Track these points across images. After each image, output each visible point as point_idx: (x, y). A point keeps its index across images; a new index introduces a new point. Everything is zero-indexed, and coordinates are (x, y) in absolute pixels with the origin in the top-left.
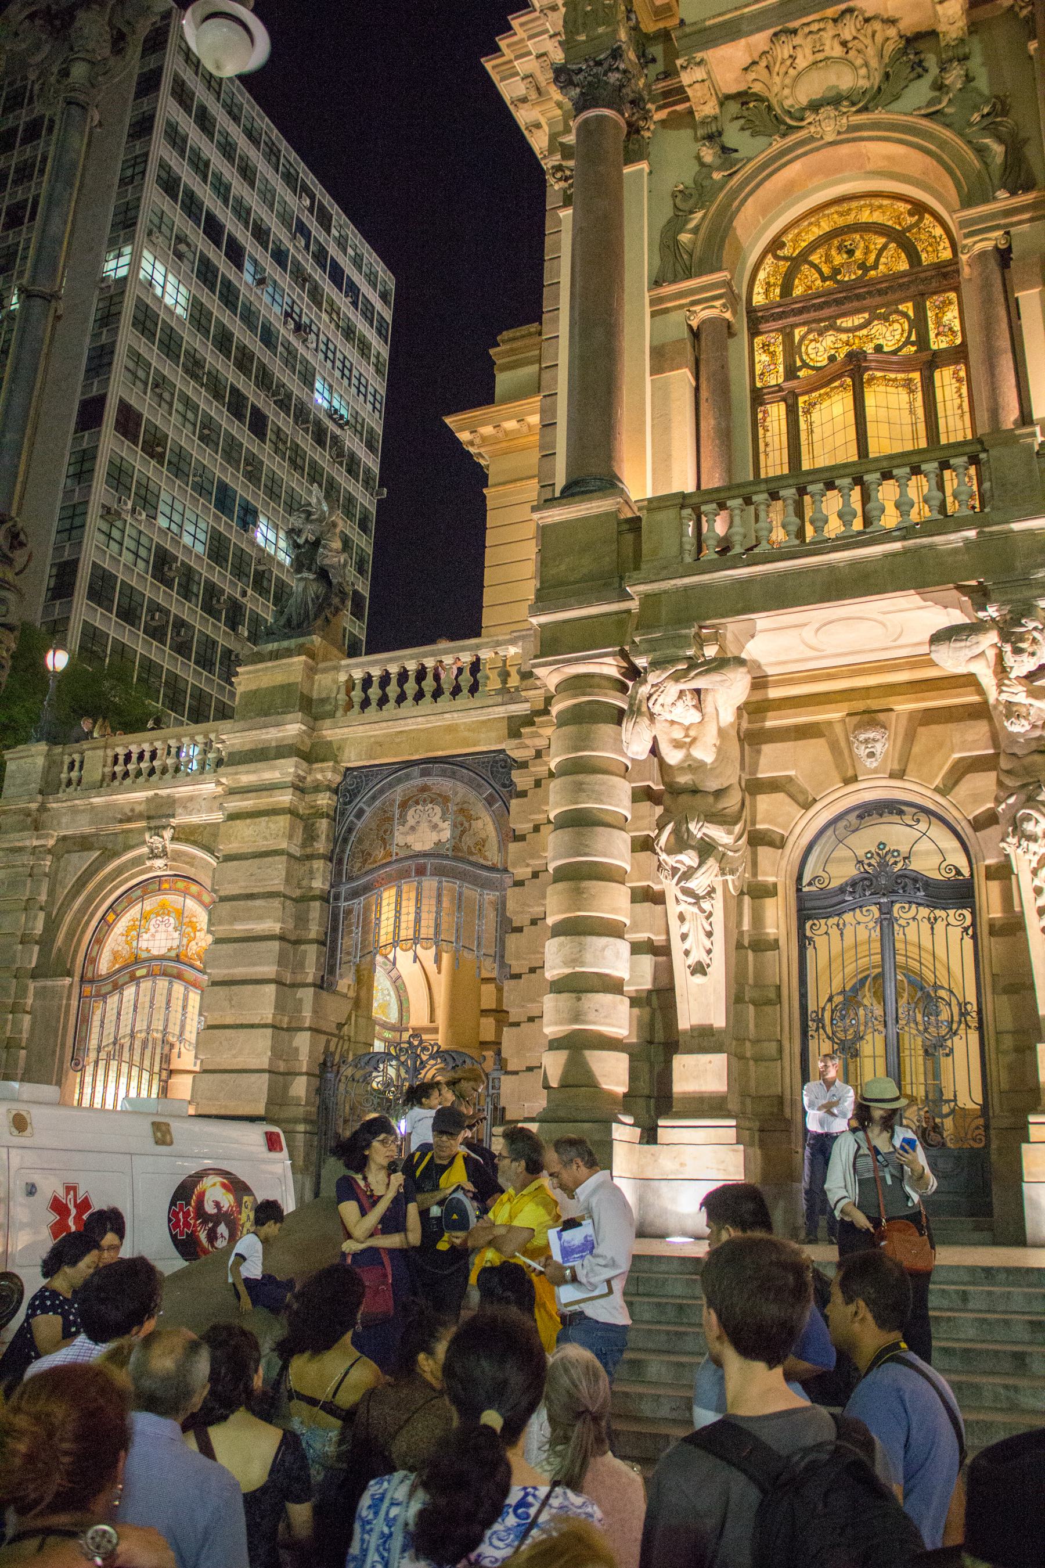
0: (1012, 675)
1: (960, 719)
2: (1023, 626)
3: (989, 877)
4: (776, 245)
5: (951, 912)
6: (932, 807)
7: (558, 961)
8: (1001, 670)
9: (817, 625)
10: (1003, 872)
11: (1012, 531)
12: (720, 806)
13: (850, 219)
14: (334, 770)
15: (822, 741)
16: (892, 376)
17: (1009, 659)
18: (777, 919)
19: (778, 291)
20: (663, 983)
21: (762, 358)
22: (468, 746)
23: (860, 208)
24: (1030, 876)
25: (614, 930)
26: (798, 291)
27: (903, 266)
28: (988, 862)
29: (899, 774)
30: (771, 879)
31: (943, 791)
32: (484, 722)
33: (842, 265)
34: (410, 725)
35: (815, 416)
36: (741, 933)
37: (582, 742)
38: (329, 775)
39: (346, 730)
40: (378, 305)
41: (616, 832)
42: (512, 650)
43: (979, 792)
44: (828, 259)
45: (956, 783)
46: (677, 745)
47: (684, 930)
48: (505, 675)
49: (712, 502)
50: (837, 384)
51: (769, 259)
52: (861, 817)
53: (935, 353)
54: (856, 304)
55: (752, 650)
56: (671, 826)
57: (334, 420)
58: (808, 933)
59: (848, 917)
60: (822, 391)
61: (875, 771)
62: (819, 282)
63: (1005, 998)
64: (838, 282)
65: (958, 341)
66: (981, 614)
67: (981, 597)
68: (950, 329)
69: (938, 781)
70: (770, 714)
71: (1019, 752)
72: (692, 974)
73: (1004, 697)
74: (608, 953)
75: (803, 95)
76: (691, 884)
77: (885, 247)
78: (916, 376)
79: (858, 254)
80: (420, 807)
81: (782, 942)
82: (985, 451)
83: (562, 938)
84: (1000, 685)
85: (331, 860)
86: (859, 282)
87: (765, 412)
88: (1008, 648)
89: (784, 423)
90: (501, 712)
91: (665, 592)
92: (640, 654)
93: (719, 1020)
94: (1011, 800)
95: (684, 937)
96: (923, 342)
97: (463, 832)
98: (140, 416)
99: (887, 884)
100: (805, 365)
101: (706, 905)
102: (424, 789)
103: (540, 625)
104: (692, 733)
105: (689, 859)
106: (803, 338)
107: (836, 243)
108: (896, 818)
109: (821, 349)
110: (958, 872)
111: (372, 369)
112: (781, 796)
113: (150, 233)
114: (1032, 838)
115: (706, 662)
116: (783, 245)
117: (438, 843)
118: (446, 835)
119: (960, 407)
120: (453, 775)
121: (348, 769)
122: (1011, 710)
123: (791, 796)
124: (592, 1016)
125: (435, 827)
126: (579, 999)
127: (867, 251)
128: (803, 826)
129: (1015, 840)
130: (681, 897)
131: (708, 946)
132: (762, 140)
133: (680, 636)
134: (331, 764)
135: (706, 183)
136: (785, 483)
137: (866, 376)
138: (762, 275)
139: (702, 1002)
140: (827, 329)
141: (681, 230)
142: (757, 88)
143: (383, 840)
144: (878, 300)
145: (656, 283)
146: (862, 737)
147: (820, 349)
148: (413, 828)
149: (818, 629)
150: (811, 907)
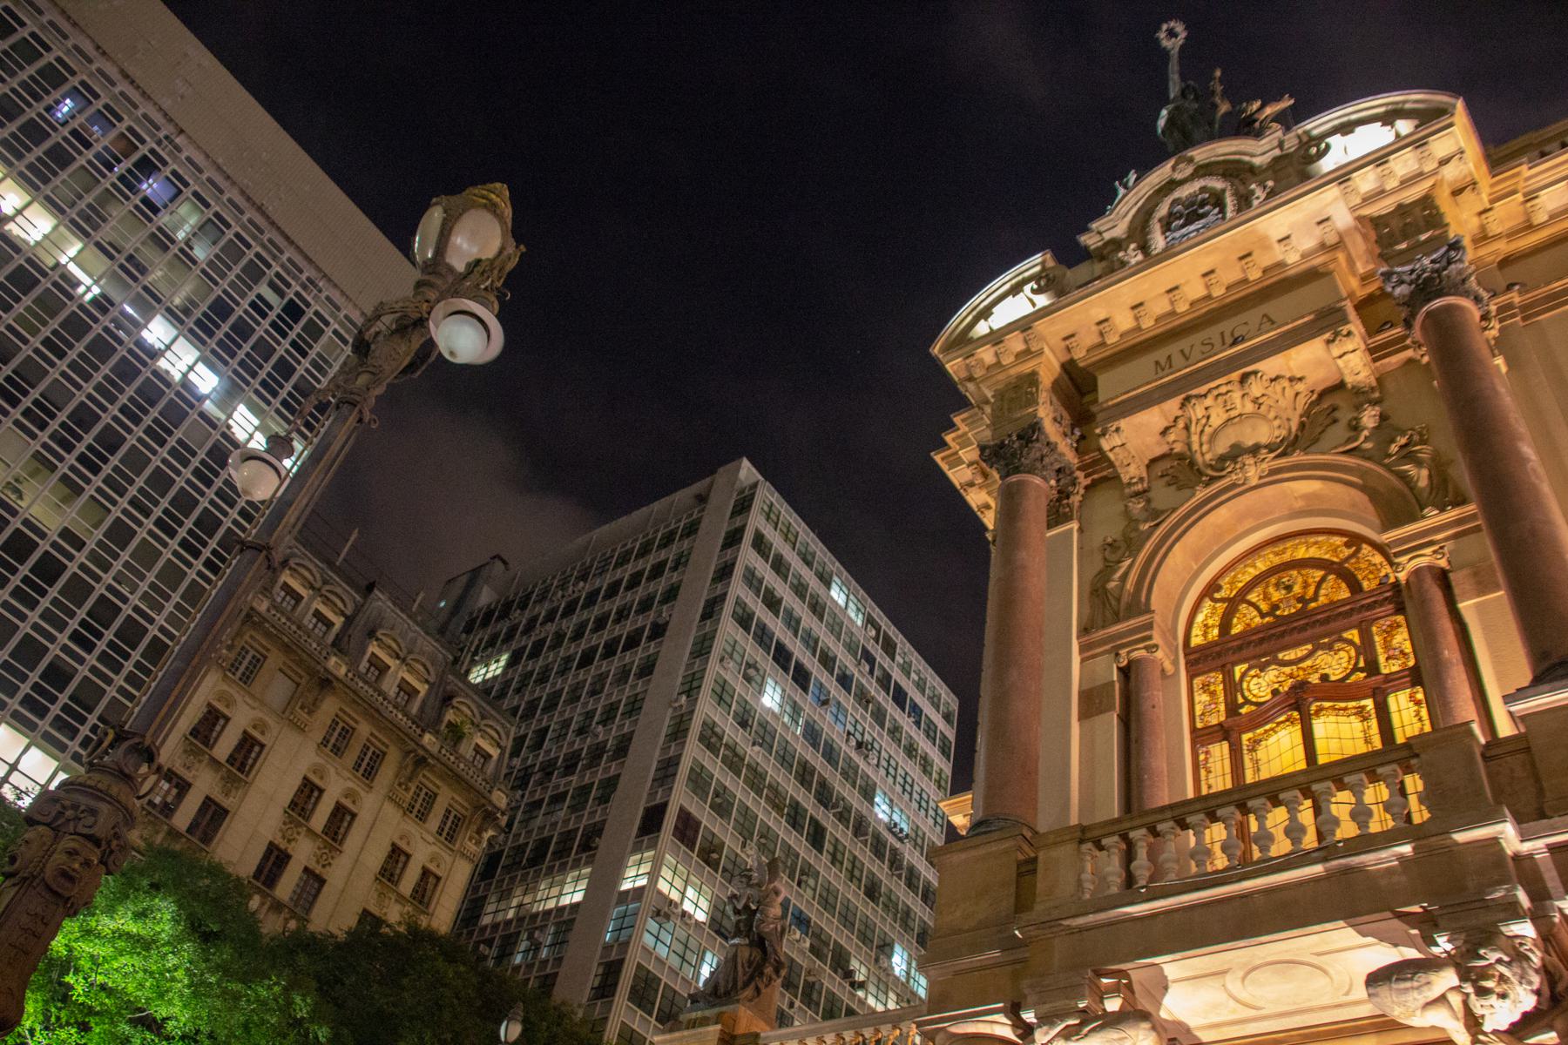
4: (1212, 588)
9: (1241, 974)
11: (1456, 844)
13: (1287, 557)
16: (1343, 705)
19: (1216, 631)
21: (1201, 698)
23: (1296, 547)
26: (1237, 629)
27: (1345, 594)
33: (1281, 601)
35: (1261, 754)
40: (941, 725)
44: (1266, 597)
49: (1113, 834)
50: (1282, 718)
51: (1208, 603)
53: (1389, 678)
54: (1296, 636)
57: (894, 834)
60: (1267, 727)
62: (1258, 620)
64: (1277, 617)
65: (1411, 663)
68: (1402, 652)
75: (1222, 447)
77: (1323, 580)
78: (1369, 703)
79: (1297, 589)
82: (1417, 756)
86: (1300, 614)
87: (1207, 753)
89: (1227, 763)
96: (1372, 668)
98: (699, 824)
100: (1247, 702)
106: (1244, 675)
107: (1273, 580)
111: (934, 787)
113: (722, 660)
116: (1219, 588)
127: (1306, 585)
132: (1187, 492)
135: (1133, 535)
136: (1192, 808)
137: (1313, 708)
138: (1200, 618)
140: (1268, 664)
141: (1108, 581)
142: (1178, 448)
144: (1318, 630)
145: (1084, 630)
147: (1260, 686)
149: (1243, 979)
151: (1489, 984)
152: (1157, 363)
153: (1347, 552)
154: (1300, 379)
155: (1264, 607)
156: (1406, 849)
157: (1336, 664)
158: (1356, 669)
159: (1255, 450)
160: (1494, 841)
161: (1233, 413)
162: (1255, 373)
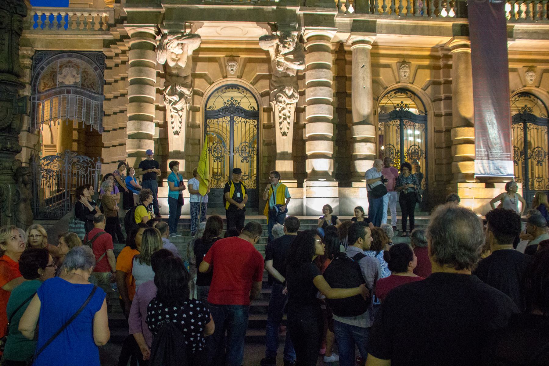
0: (281, 53)
1: (259, 62)
3: (264, 111)
5: (251, 120)
6: (248, 88)
7: (133, 128)
8: (277, 51)
10: (269, 110)
12: (186, 82)
14: (31, 50)
15: (217, 64)
17: (281, 48)
18: (199, 119)
20: (163, 136)
22: (87, 48)
25: (150, 119)
28: (265, 107)
29: (240, 77)
30: (198, 106)
31: (253, 84)
32: (94, 40)
34: (64, 37)
36: (189, 122)
37: (143, 56)
38: (30, 52)
39: (36, 35)
41: (152, 87)
42: (104, 15)
43: (264, 86)
45: (257, 82)
46: (174, 60)
47: (173, 120)
48: (101, 24)
52: (226, 89)
55: (199, 32)
56: (170, 87)
58: (208, 124)
59: (220, 119)
61: (233, 75)
63: (266, 147)
66: (274, 33)
67: (275, 28)
69: (251, 81)
70: (201, 52)
71: (278, 75)
72: (175, 134)
73: (277, 59)
74: (149, 127)
76: (176, 106)
80: (67, 68)
81: (201, 126)
83: (134, 121)
84: (276, 55)
85: (31, 85)
88: (282, 45)
90: (101, 37)
91: (175, 8)
92: (165, 28)
93: (182, 149)
94: (275, 90)
95: (172, 123)
97: (85, 79)
99: (232, 110)
101: (180, 113)
102: (69, 62)
103: (127, 12)
104: (179, 57)
105: (176, 98)
108: (236, 90)
110: (254, 109)
112: (203, 79)
114: (281, 102)
115: (187, 35)
117: (75, 83)
118: (79, 80)
120: (81, 58)
121: (36, 51)
122: (279, 64)
123: (206, 80)
124: (144, 147)
125: (74, 76)
126: (140, 141)
128: (209, 89)
129: (275, 102)
130: (172, 110)
131: (180, 126)
133: (180, 25)
134: (30, 48)
139: (177, 143)
143: (53, 80)
146: (230, 64)
148: (65, 76)
150: (209, 115)
151: (286, 45)
156: (275, 7)
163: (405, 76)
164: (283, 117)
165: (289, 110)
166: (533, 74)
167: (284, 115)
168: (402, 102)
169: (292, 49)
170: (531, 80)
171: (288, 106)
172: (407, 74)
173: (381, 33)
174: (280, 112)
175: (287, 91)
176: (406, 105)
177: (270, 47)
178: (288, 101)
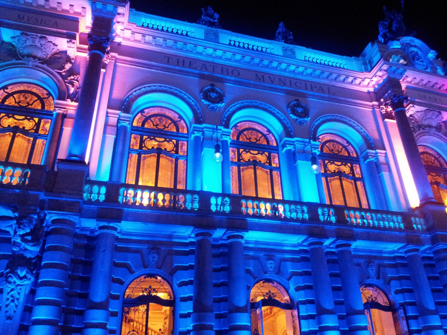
0: (18, 234)
2: (23, 221)
8: (15, 232)
16: (25, 137)
23: (34, 87)
24: (6, 294)
26: (6, 103)
27: (39, 108)
33: (22, 101)
62: (14, 103)
75: (26, 52)
79: (28, 100)
88: (17, 226)
96: (37, 131)
109: (7, 122)
114: (10, 283)
116: (7, 89)
119: (41, 151)
122: (15, 244)
127: (31, 100)
137: (17, 134)
152: (19, 16)
153: (46, 96)
154: (57, 45)
155: (17, 100)
157: (28, 125)
158: (33, 129)
159: (35, 57)
160: (38, 195)
161: (34, 44)
162: (45, 37)
163: (153, 261)
164: (11, 299)
165: (19, 291)
166: (272, 262)
167: (12, 296)
168: (150, 287)
169: (28, 231)
170: (271, 267)
171: (19, 287)
172: (156, 260)
173: (127, 220)
174: (8, 293)
175: (19, 272)
176: (154, 290)
177: (9, 227)
178: (18, 282)
